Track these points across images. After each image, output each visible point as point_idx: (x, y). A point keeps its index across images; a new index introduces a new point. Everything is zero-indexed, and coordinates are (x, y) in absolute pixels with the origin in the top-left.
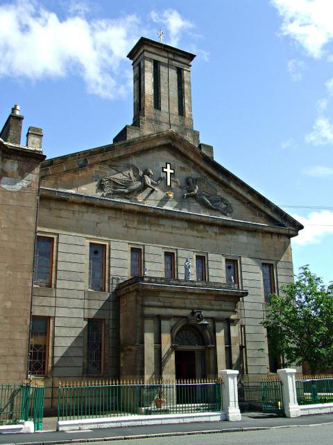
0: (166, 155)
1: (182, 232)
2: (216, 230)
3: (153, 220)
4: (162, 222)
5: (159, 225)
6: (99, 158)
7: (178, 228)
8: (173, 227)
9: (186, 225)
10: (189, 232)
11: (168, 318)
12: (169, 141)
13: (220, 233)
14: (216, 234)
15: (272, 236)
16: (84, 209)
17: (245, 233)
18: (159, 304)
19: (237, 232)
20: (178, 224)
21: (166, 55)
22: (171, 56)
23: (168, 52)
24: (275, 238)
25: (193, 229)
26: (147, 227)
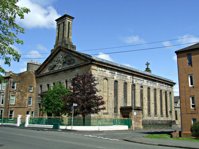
0: (61, 53)
2: (70, 70)
4: (59, 73)
5: (58, 75)
6: (47, 62)
9: (63, 72)
10: (64, 74)
13: (71, 71)
14: (70, 72)
20: (62, 73)
21: (61, 20)
22: (62, 20)
23: (61, 19)
24: (86, 66)
25: (65, 73)
26: (56, 76)
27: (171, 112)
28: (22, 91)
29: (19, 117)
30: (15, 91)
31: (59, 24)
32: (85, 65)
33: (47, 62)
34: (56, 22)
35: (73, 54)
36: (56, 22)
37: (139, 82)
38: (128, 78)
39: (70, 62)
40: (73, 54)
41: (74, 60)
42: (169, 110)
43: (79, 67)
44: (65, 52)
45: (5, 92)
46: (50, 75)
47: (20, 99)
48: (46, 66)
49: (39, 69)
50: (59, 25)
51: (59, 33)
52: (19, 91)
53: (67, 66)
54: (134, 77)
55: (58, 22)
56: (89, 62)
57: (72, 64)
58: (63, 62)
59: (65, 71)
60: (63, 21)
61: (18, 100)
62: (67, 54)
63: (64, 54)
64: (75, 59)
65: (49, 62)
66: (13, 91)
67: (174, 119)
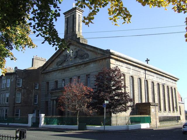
1: (74, 70)
2: (83, 66)
3: (67, 69)
4: (70, 69)
6: (55, 57)
7: (73, 69)
8: (72, 70)
9: (75, 67)
11: (55, 99)
12: (70, 42)
13: (85, 66)
15: (105, 60)
16: (54, 72)
17: (93, 63)
18: (54, 96)
19: (90, 64)
20: (73, 68)
21: (70, 13)
22: (71, 12)
24: (104, 60)
25: (76, 68)
27: (176, 108)
28: (28, 88)
29: (30, 116)
30: (20, 88)
31: (67, 17)
32: (102, 59)
33: (55, 57)
34: (64, 16)
35: (87, 47)
36: (64, 16)
37: (151, 78)
38: (141, 73)
39: (82, 57)
40: (87, 47)
41: (88, 55)
42: (175, 106)
43: (94, 61)
44: (76, 46)
45: (9, 89)
46: (58, 71)
47: (26, 97)
48: (53, 61)
49: (45, 64)
50: (68, 18)
51: (69, 27)
52: (25, 88)
53: (79, 61)
54: (147, 72)
55: (67, 15)
56: (107, 56)
57: (86, 59)
58: (74, 57)
59: (76, 66)
60: (73, 14)
61: (24, 98)
62: (78, 48)
63: (75, 49)
64: (89, 53)
65: (57, 57)
66: (19, 88)
67: (179, 115)
